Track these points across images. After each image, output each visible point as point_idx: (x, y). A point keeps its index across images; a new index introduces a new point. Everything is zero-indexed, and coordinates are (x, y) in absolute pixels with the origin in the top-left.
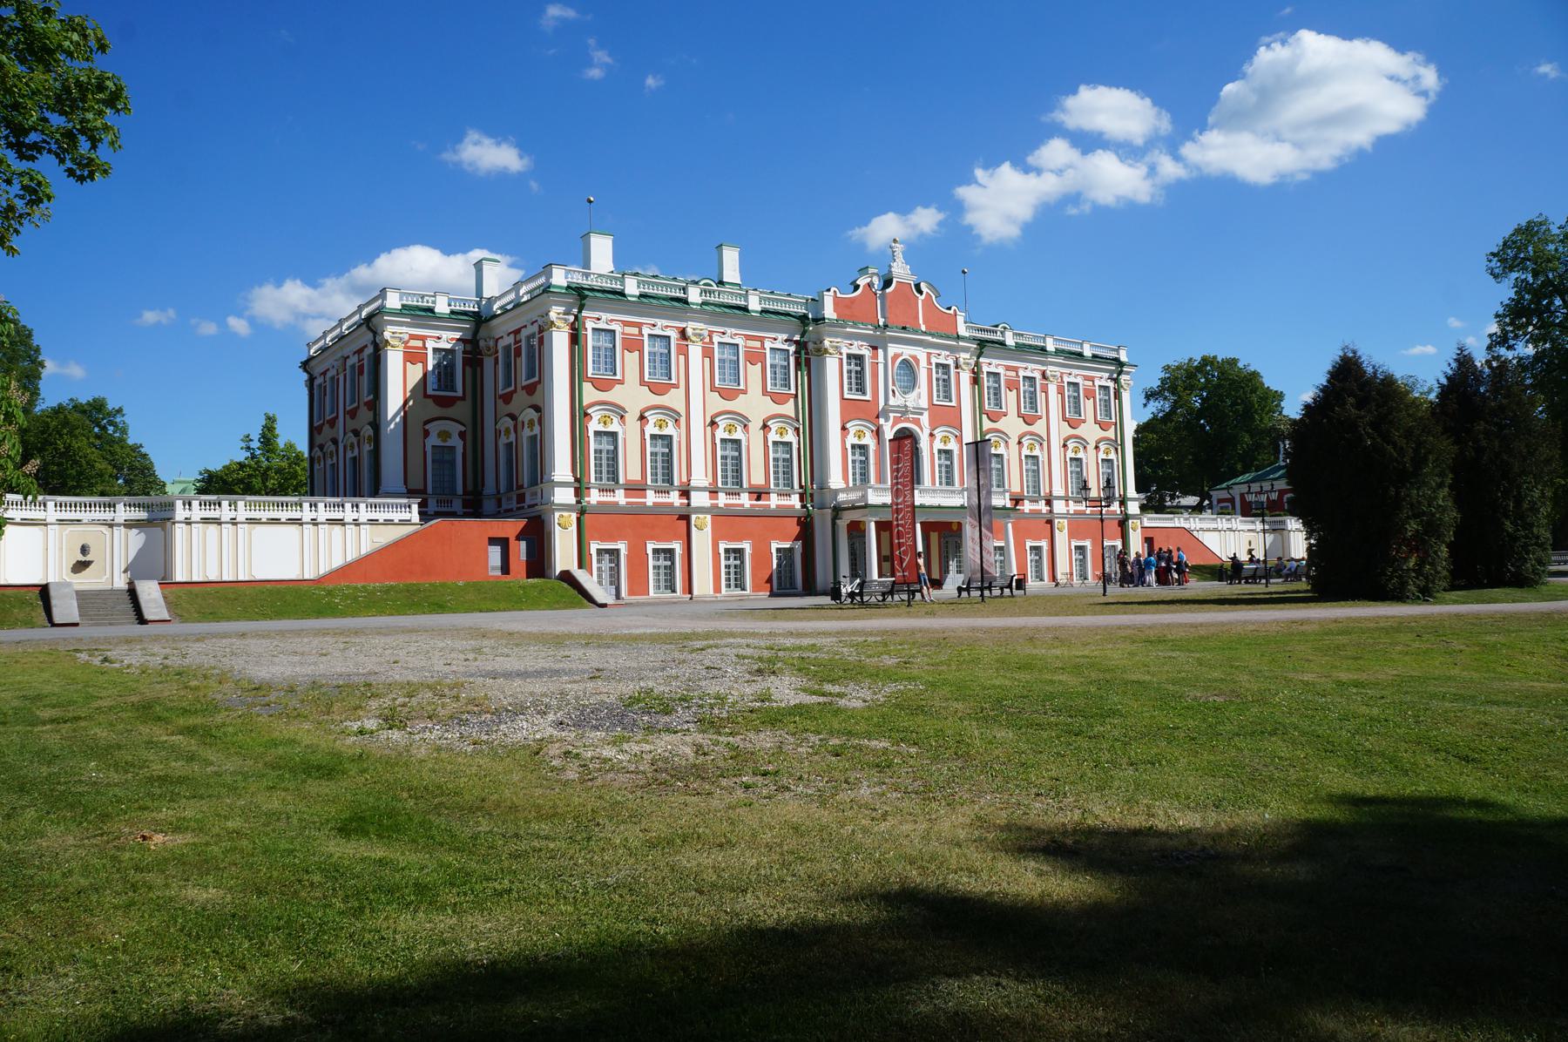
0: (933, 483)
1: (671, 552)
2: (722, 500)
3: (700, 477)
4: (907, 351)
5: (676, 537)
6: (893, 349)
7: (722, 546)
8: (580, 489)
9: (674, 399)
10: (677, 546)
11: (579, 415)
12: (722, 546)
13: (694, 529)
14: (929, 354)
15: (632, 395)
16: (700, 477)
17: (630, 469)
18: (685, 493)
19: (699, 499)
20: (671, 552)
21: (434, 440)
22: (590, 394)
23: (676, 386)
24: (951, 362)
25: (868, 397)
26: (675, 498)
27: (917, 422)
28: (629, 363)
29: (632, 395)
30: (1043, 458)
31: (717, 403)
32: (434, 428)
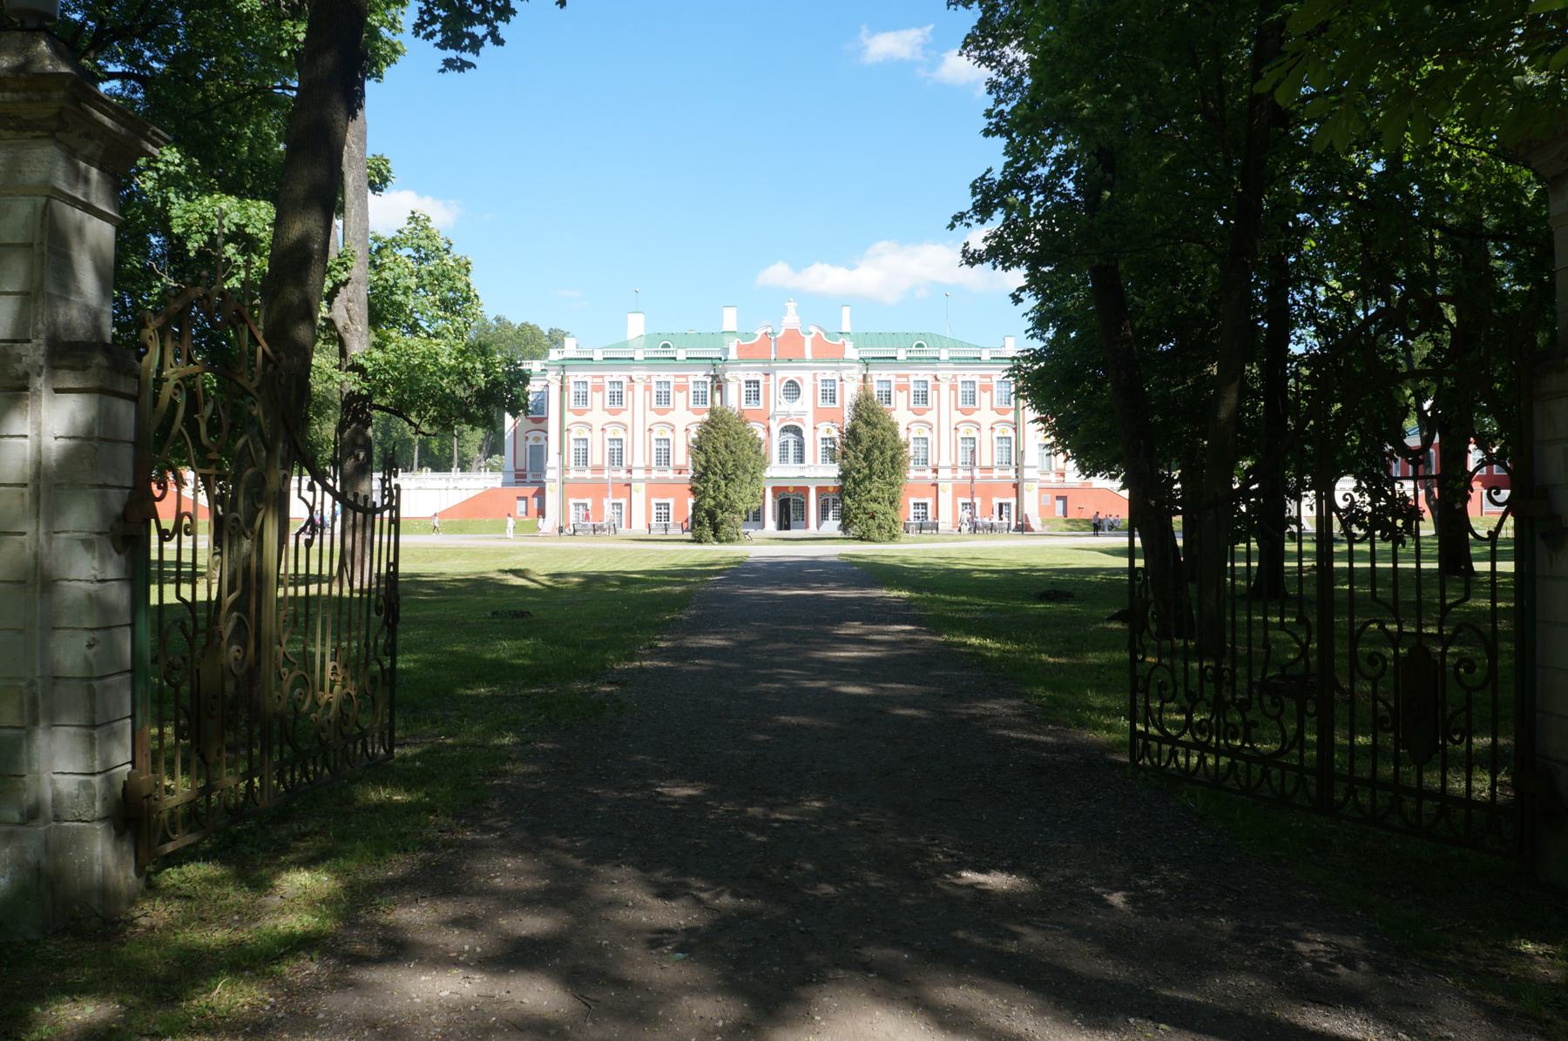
0: (815, 461)
1: (925, 505)
2: (655, 474)
5: (622, 496)
6: (780, 374)
7: (654, 501)
8: (564, 469)
9: (624, 417)
17: (596, 458)
20: (925, 505)
21: (531, 442)
27: (801, 420)
28: (596, 399)
29: (597, 413)
30: (932, 438)
31: (653, 417)
32: (531, 435)
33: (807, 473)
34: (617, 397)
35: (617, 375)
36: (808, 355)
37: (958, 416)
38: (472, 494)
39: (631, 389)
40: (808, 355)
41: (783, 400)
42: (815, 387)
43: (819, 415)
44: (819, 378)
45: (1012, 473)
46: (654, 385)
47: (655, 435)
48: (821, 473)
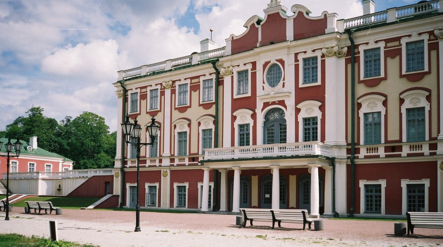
3: (167, 152)
12: (176, 185)
13: (162, 177)
16: (167, 152)
18: (161, 161)
23: (160, 111)
25: (249, 94)
27: (282, 103)
31: (177, 114)
39: (163, 94)
41: (266, 85)
42: (297, 67)
44: (301, 57)
46: (177, 88)
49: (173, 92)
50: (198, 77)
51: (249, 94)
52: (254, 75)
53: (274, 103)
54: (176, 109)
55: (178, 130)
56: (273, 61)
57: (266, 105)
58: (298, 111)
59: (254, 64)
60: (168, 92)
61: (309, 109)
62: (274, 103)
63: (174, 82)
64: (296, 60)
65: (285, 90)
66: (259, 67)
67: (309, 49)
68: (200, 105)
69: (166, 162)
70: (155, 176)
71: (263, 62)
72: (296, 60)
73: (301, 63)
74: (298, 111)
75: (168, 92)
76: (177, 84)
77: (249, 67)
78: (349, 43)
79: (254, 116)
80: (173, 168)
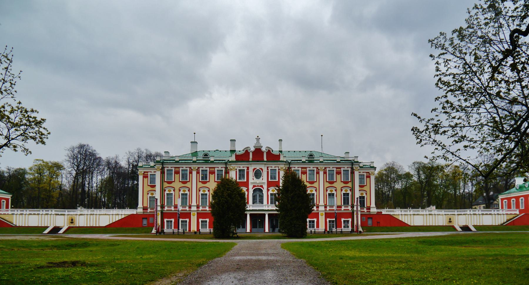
0: (268, 203)
3: (194, 203)
4: (258, 167)
8: (162, 207)
9: (188, 185)
10: (188, 220)
11: (163, 190)
12: (200, 220)
14: (268, 167)
15: (177, 185)
16: (194, 203)
18: (190, 207)
19: (194, 208)
22: (166, 185)
24: (277, 169)
25: (245, 181)
26: (187, 208)
27: (262, 186)
29: (177, 185)
33: (264, 208)
34: (184, 176)
35: (184, 167)
36: (265, 159)
37: (327, 185)
38: (123, 217)
39: (191, 173)
40: (265, 159)
41: (254, 178)
42: (268, 172)
43: (270, 184)
44: (269, 169)
45: (350, 208)
47: (201, 192)
48: (270, 208)
49: (198, 173)
50: (214, 168)
51: (245, 181)
52: (248, 173)
53: (258, 186)
54: (200, 182)
55: (201, 192)
56: (258, 168)
57: (254, 186)
58: (268, 190)
59: (248, 168)
60: (194, 173)
61: (273, 191)
62: (258, 186)
63: (199, 168)
64: (268, 169)
65: (263, 181)
66: (251, 170)
67: (273, 166)
68: (215, 181)
69: (194, 208)
70: (188, 215)
71: (253, 168)
72: (268, 169)
73: (269, 171)
74: (268, 190)
75: (194, 173)
76: (201, 169)
77: (246, 169)
78: (288, 166)
79: (248, 190)
80: (199, 212)
